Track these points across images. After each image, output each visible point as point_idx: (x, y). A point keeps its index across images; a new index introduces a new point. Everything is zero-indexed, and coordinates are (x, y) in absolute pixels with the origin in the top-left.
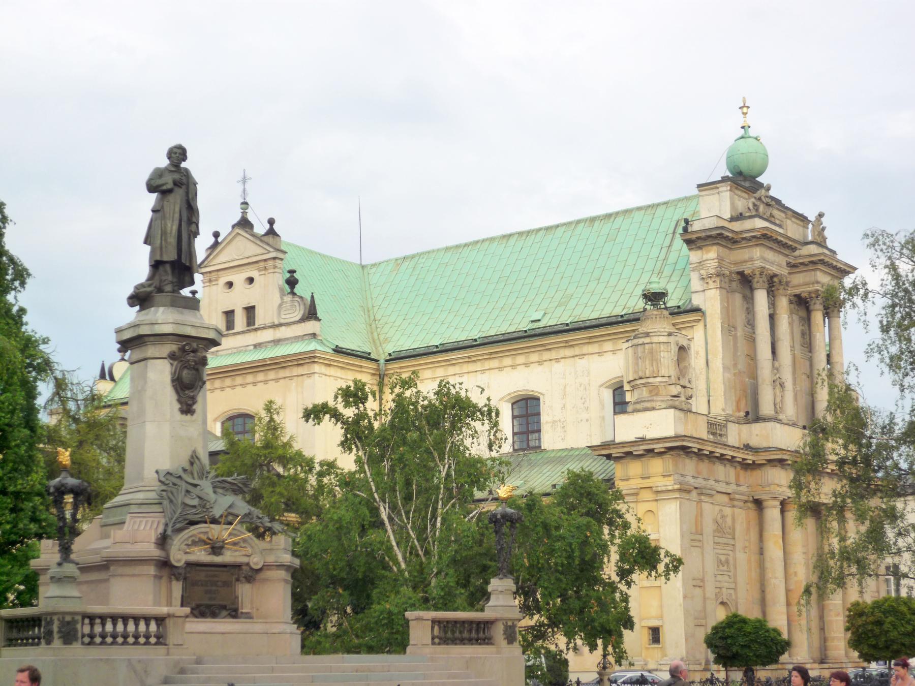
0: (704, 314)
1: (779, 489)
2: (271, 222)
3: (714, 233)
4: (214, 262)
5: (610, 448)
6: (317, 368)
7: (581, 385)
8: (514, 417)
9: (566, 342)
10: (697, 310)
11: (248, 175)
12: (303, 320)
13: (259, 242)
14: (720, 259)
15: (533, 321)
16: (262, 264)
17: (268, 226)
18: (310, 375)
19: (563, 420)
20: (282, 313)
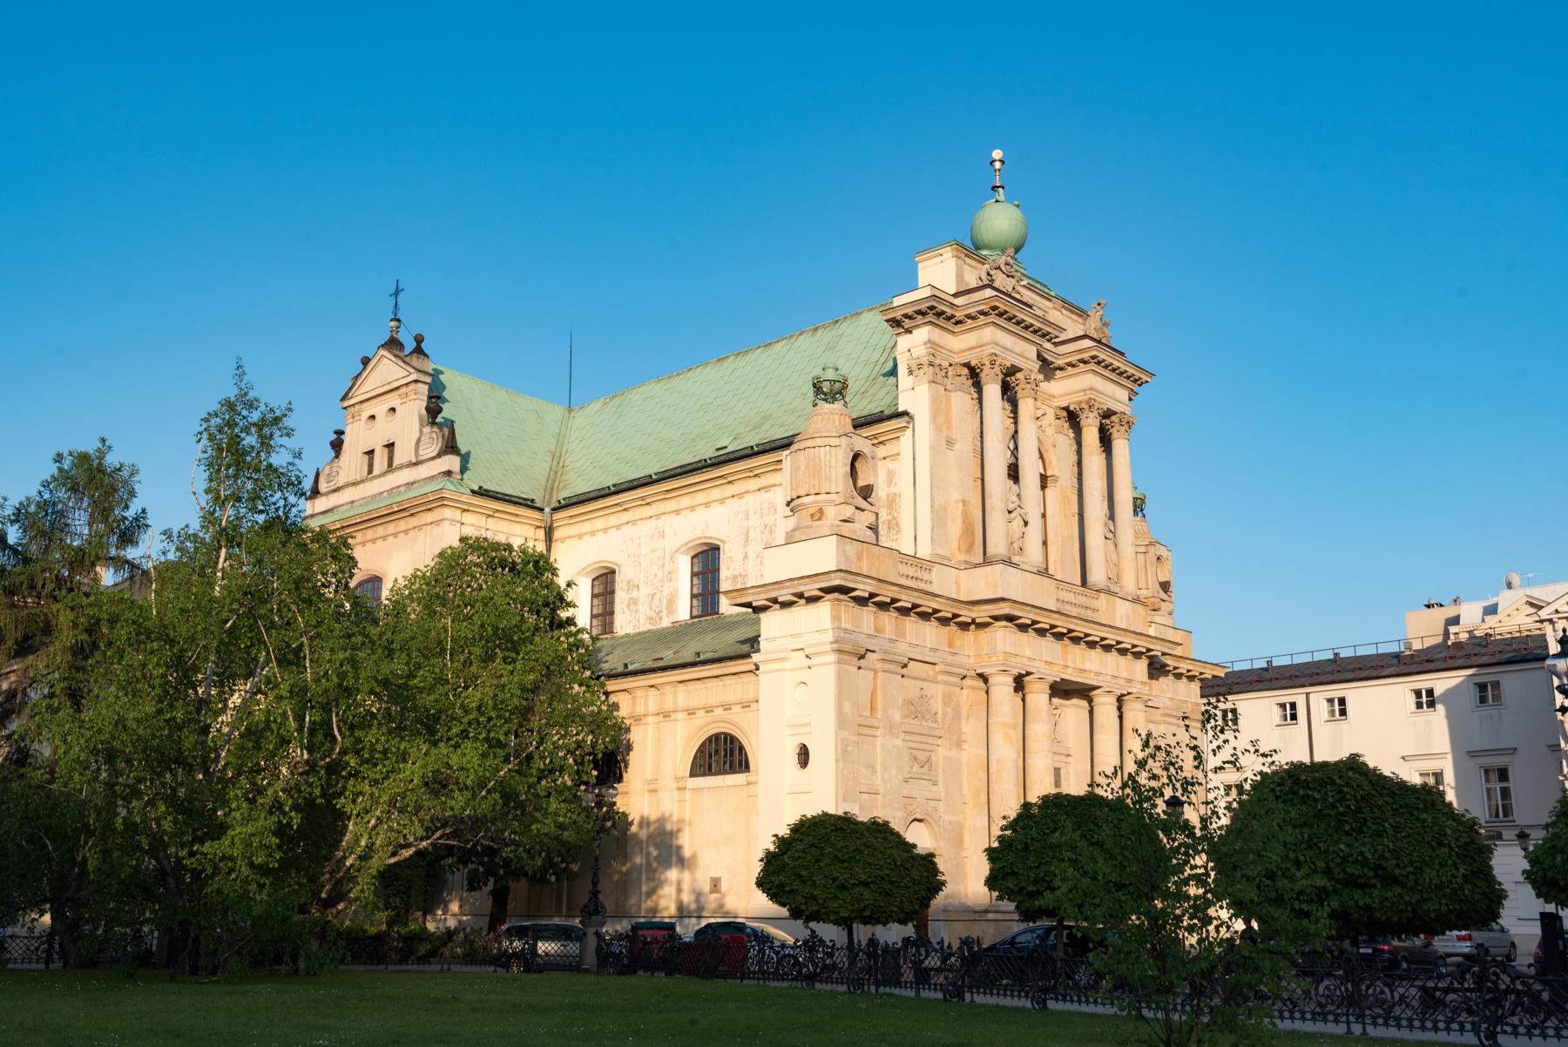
0: (912, 418)
1: (1014, 660)
2: (419, 340)
3: (923, 307)
4: (359, 392)
5: (748, 594)
6: (447, 513)
7: (766, 527)
8: (693, 575)
9: (750, 469)
10: (905, 413)
11: (401, 286)
12: (439, 456)
13: (402, 364)
14: (931, 343)
15: (718, 449)
16: (403, 390)
17: (414, 344)
18: (438, 522)
19: (743, 574)
20: (421, 448)
